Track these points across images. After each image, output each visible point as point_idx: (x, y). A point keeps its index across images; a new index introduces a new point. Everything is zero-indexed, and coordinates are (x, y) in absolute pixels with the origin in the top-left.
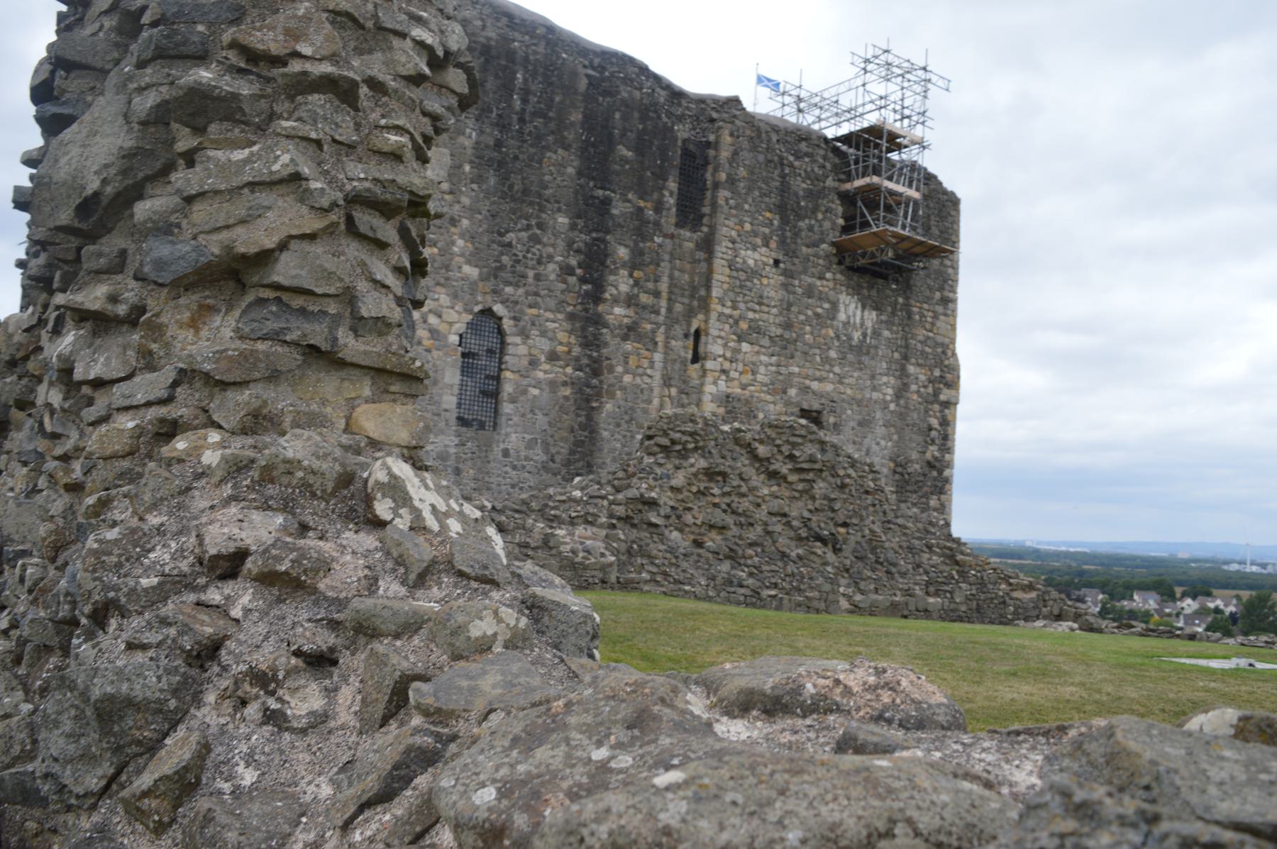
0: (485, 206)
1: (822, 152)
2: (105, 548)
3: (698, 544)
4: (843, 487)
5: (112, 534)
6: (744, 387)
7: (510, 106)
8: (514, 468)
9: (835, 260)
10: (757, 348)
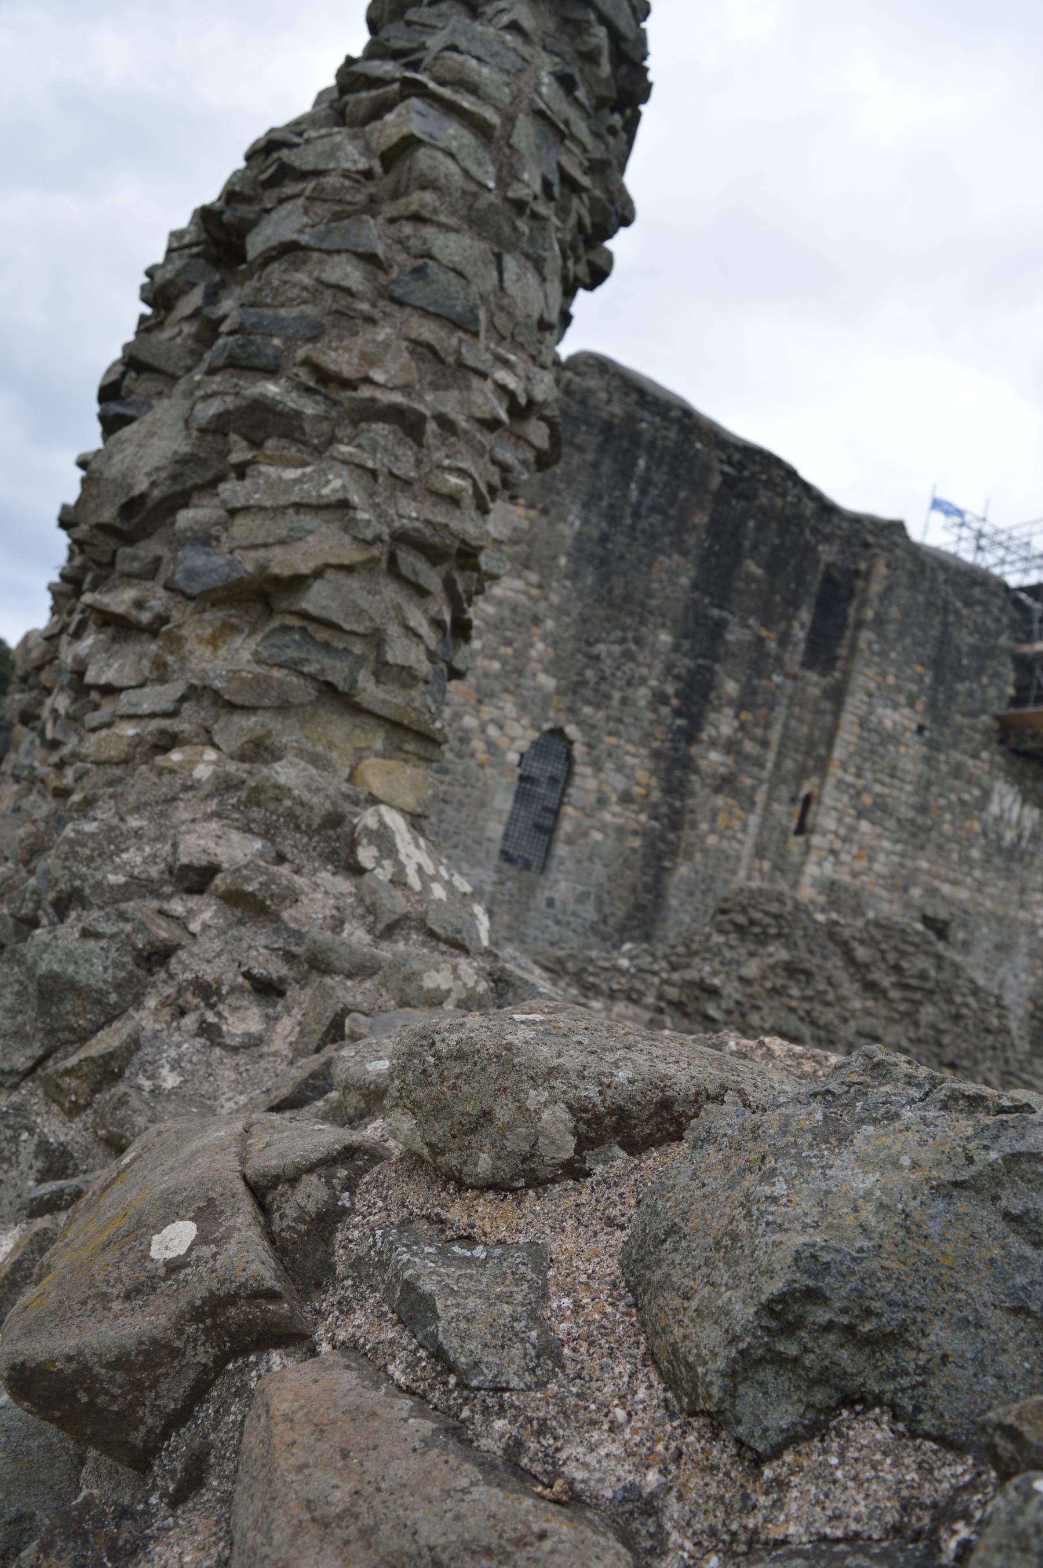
0: (576, 609)
2: (82, 838)
4: (957, 1018)
5: (90, 827)
6: (855, 875)
7: (625, 496)
8: (558, 922)
9: (996, 737)
10: (878, 830)
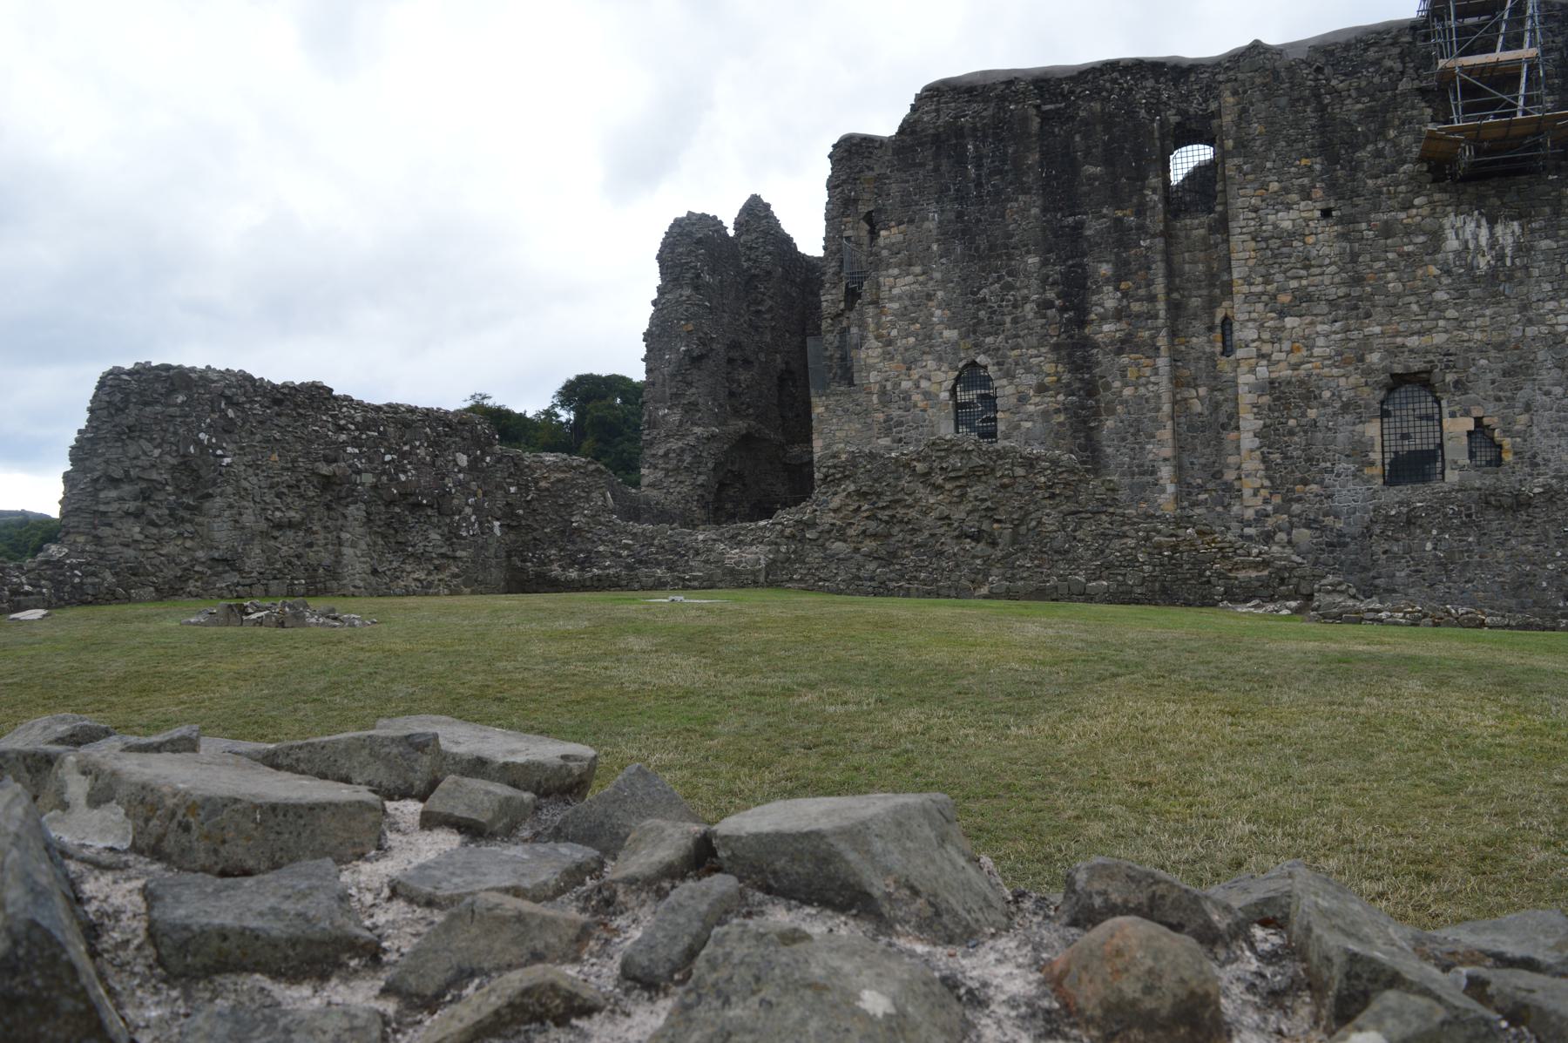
1: (1396, 50)
3: (857, 550)
4: (1004, 486)
10: (1308, 319)
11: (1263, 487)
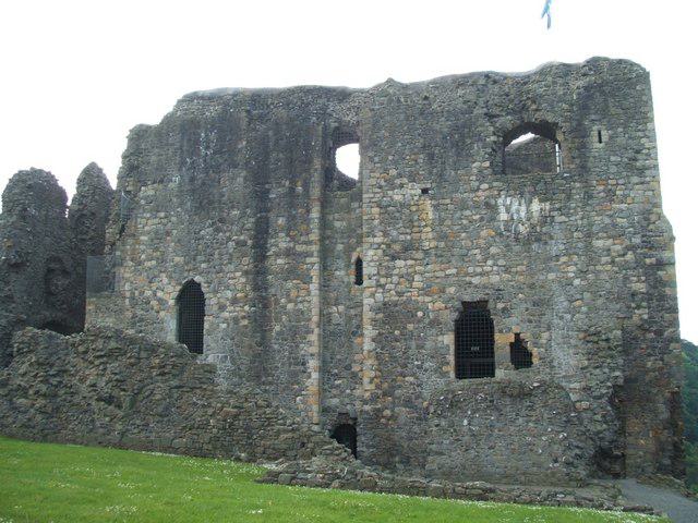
6: (400, 294)
10: (410, 262)
11: (376, 377)
